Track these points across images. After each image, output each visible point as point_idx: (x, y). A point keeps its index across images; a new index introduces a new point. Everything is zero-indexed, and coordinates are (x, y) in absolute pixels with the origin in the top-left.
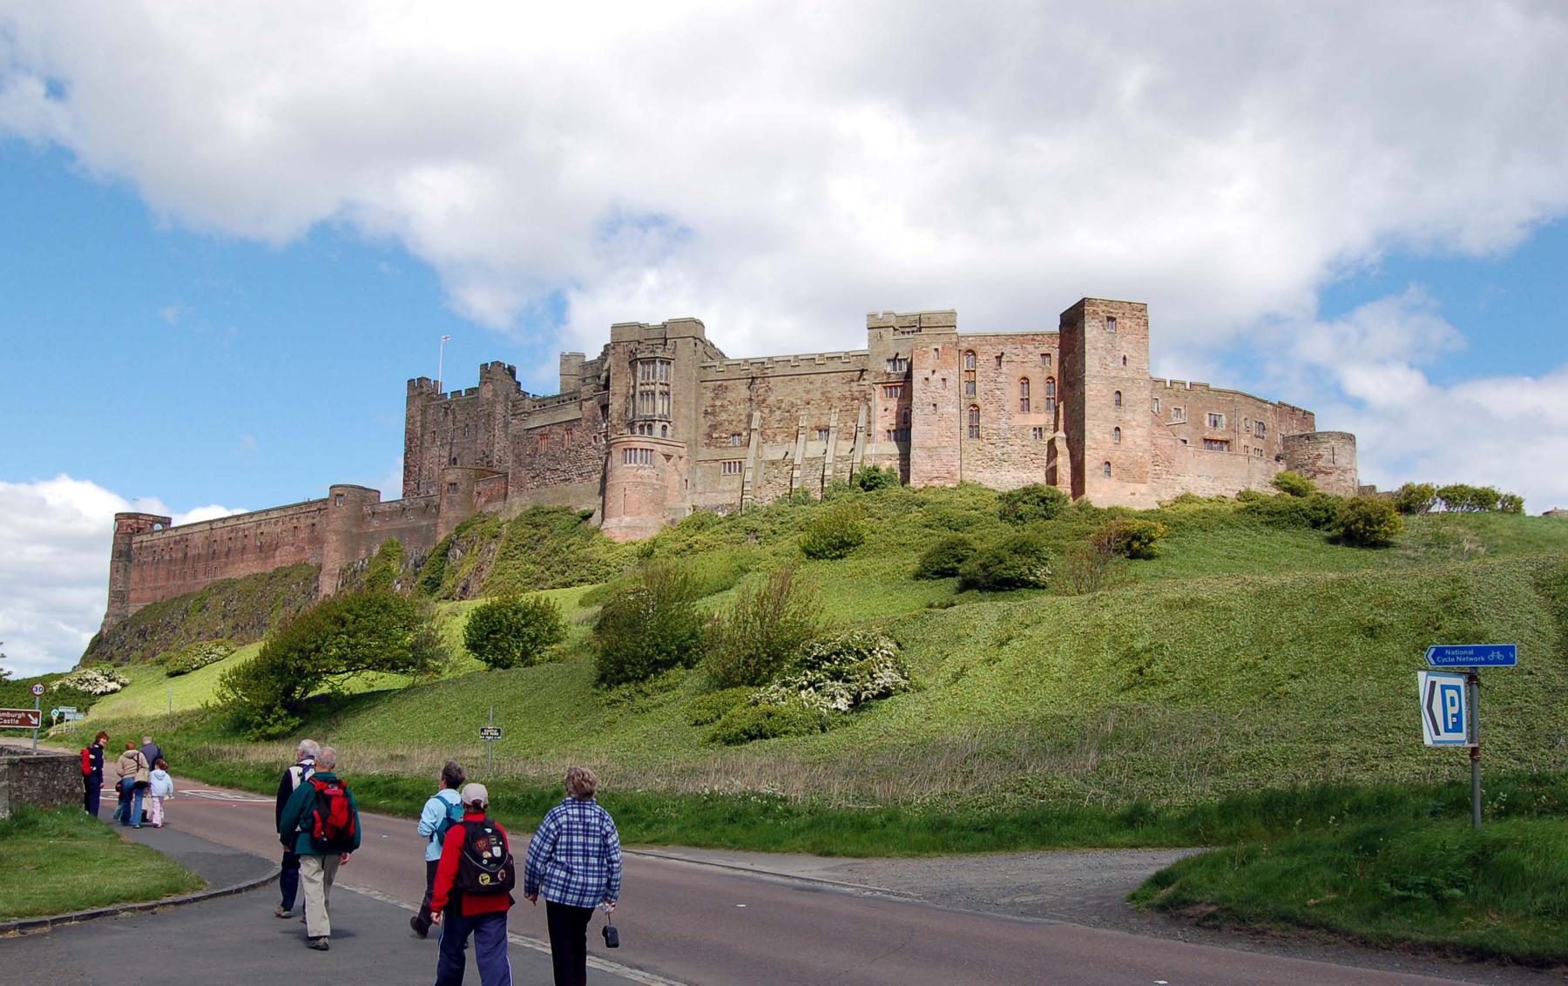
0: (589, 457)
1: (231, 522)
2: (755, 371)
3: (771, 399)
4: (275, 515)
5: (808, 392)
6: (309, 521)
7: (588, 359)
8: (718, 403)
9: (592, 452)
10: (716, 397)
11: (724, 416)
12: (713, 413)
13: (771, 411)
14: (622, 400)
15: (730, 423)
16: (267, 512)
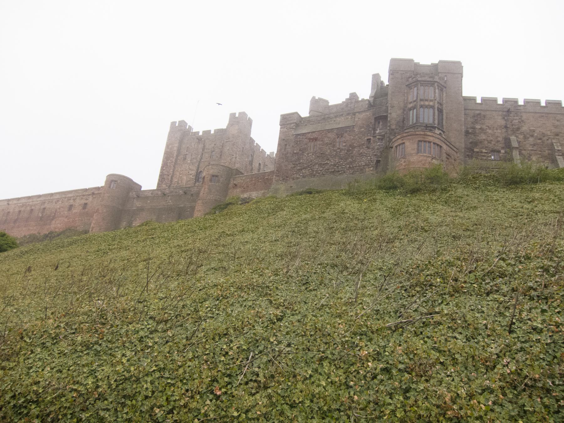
0: (361, 155)
1: (23, 201)
2: (508, 106)
3: (525, 128)
4: (58, 196)
5: (556, 127)
6: (83, 201)
7: (330, 104)
8: (478, 127)
9: (364, 150)
10: (476, 122)
11: (483, 137)
12: (474, 133)
13: (525, 138)
14: (399, 112)
15: (490, 142)
16: (52, 195)
